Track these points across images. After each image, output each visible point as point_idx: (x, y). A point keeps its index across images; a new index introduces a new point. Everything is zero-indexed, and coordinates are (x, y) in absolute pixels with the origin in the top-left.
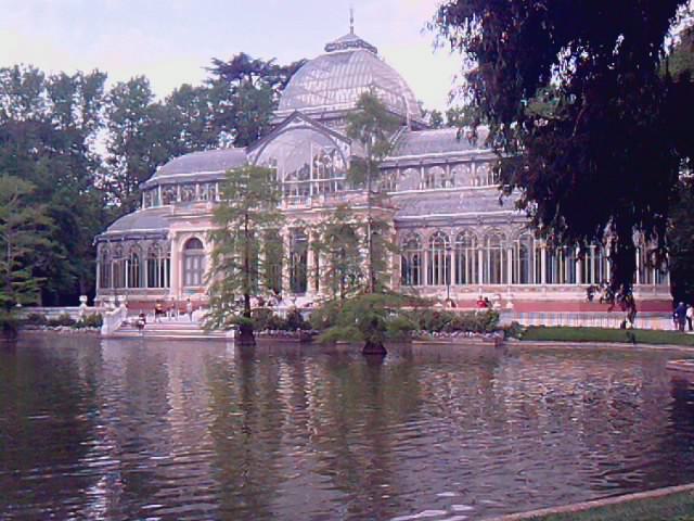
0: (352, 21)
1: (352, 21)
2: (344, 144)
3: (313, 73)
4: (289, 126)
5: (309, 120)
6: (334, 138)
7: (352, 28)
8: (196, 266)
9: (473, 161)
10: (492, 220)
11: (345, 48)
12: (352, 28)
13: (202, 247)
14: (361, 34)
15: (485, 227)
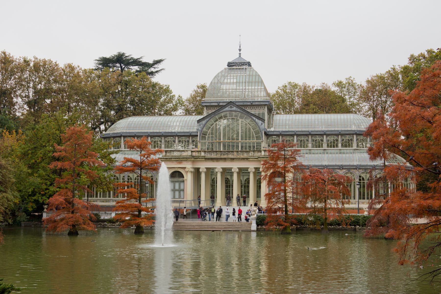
0: (240, 50)
1: (240, 50)
2: (260, 121)
3: (226, 80)
4: (225, 110)
5: (238, 106)
6: (254, 118)
7: (240, 54)
8: (182, 188)
9: (325, 134)
10: (348, 167)
11: (241, 66)
12: (240, 54)
13: (183, 177)
14: (246, 58)
15: (344, 170)
